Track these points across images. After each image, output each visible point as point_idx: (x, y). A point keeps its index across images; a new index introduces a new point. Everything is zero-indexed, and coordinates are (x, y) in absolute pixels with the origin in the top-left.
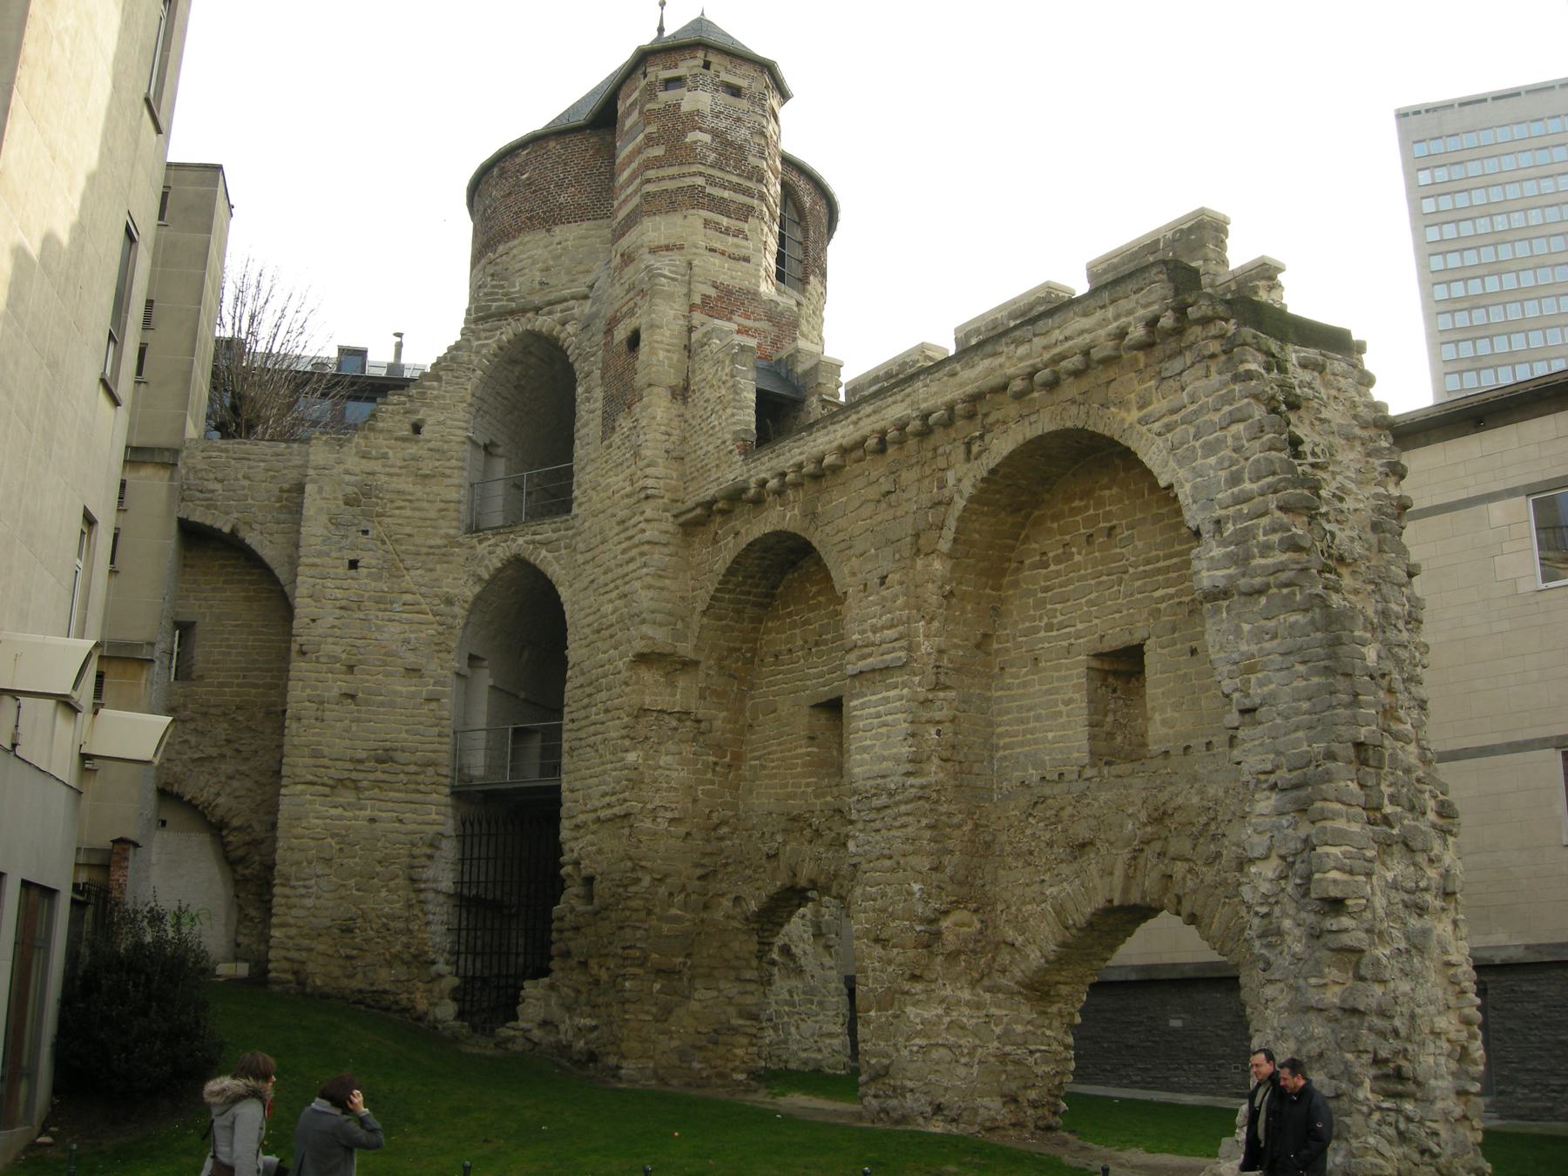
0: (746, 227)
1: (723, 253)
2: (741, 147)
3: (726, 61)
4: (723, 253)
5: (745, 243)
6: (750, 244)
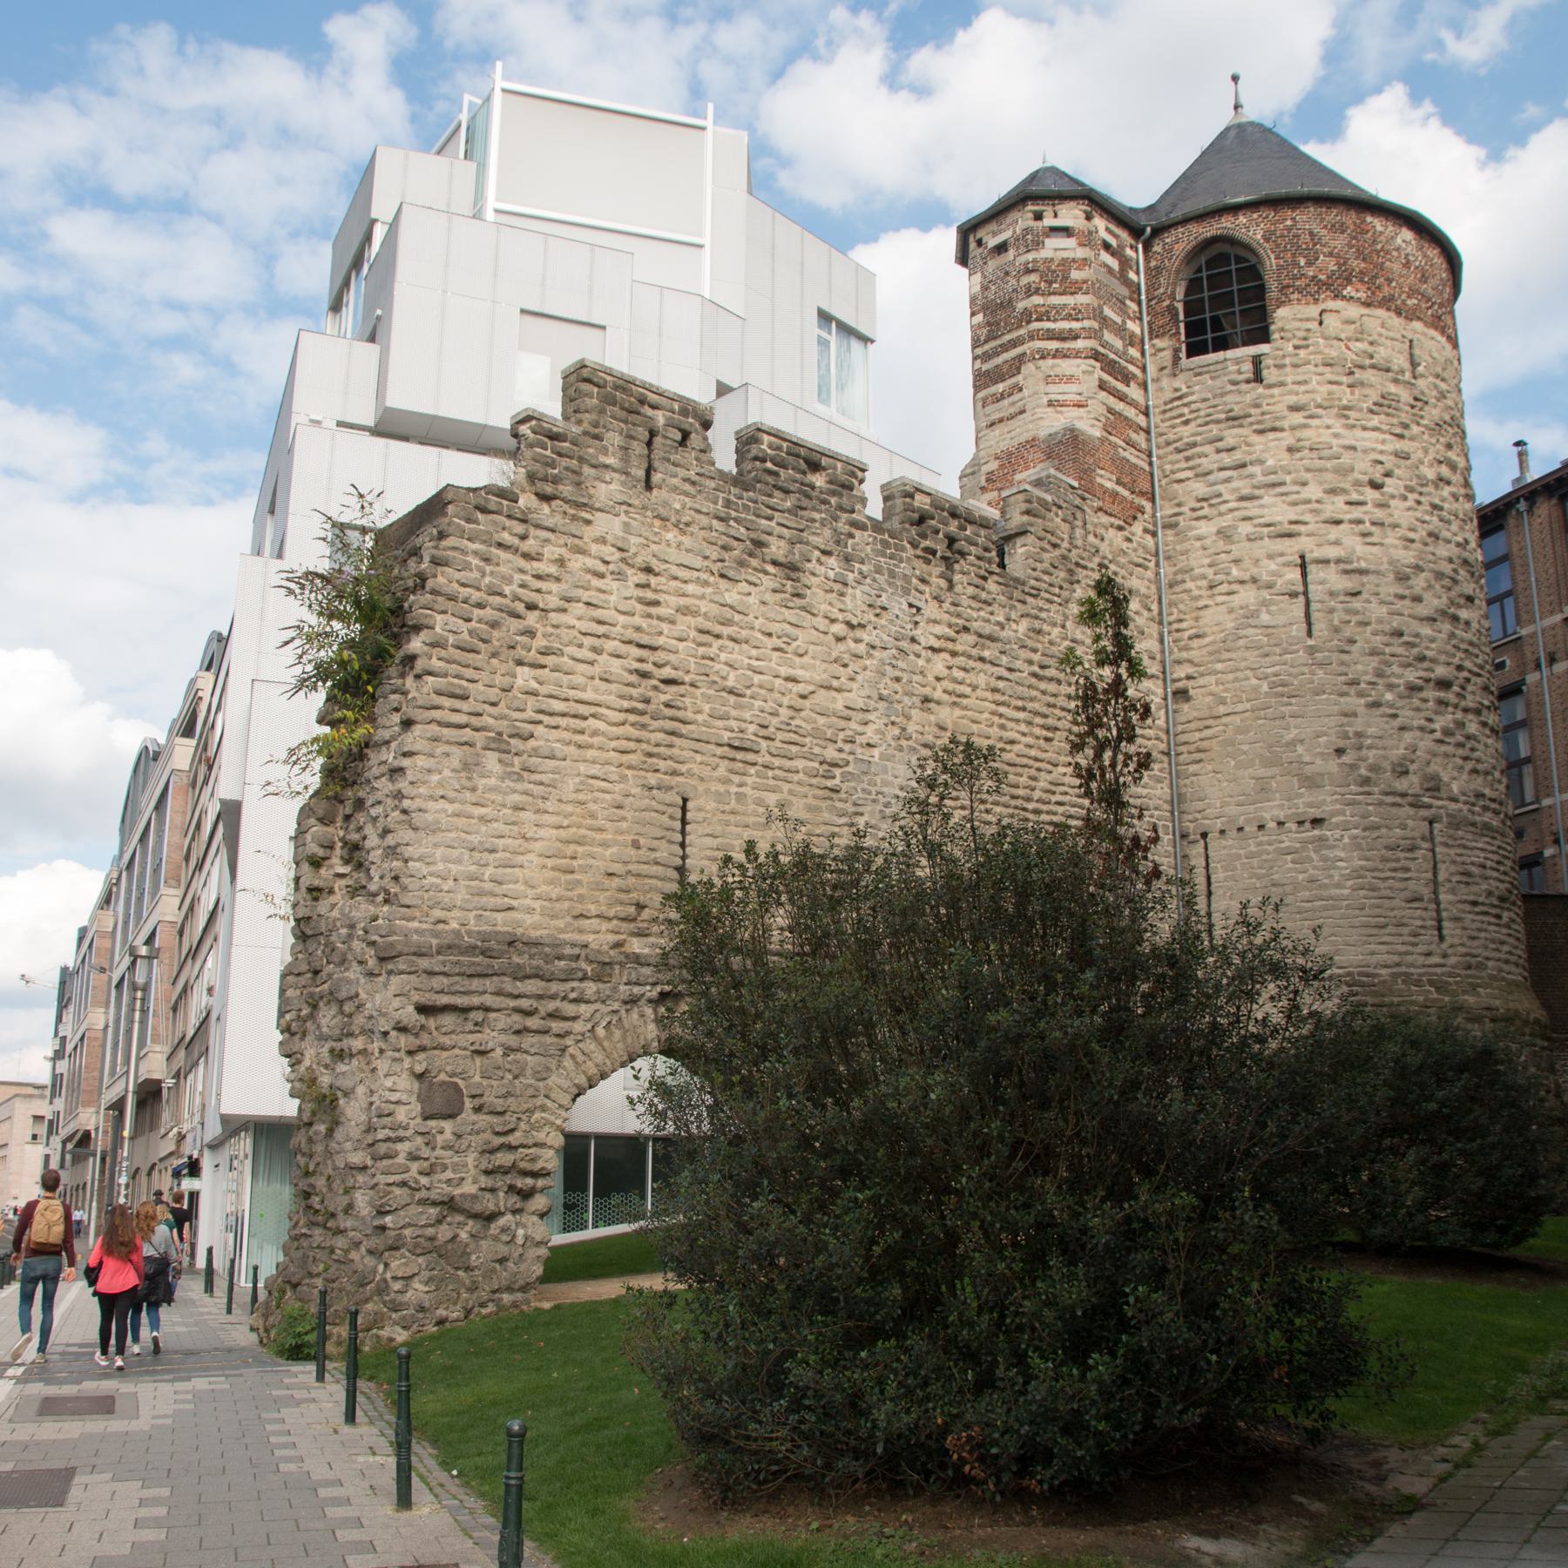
0: (1020, 378)
1: (1001, 421)
2: (1010, 301)
3: (993, 226)
4: (1001, 421)
5: (1020, 395)
6: (1026, 392)
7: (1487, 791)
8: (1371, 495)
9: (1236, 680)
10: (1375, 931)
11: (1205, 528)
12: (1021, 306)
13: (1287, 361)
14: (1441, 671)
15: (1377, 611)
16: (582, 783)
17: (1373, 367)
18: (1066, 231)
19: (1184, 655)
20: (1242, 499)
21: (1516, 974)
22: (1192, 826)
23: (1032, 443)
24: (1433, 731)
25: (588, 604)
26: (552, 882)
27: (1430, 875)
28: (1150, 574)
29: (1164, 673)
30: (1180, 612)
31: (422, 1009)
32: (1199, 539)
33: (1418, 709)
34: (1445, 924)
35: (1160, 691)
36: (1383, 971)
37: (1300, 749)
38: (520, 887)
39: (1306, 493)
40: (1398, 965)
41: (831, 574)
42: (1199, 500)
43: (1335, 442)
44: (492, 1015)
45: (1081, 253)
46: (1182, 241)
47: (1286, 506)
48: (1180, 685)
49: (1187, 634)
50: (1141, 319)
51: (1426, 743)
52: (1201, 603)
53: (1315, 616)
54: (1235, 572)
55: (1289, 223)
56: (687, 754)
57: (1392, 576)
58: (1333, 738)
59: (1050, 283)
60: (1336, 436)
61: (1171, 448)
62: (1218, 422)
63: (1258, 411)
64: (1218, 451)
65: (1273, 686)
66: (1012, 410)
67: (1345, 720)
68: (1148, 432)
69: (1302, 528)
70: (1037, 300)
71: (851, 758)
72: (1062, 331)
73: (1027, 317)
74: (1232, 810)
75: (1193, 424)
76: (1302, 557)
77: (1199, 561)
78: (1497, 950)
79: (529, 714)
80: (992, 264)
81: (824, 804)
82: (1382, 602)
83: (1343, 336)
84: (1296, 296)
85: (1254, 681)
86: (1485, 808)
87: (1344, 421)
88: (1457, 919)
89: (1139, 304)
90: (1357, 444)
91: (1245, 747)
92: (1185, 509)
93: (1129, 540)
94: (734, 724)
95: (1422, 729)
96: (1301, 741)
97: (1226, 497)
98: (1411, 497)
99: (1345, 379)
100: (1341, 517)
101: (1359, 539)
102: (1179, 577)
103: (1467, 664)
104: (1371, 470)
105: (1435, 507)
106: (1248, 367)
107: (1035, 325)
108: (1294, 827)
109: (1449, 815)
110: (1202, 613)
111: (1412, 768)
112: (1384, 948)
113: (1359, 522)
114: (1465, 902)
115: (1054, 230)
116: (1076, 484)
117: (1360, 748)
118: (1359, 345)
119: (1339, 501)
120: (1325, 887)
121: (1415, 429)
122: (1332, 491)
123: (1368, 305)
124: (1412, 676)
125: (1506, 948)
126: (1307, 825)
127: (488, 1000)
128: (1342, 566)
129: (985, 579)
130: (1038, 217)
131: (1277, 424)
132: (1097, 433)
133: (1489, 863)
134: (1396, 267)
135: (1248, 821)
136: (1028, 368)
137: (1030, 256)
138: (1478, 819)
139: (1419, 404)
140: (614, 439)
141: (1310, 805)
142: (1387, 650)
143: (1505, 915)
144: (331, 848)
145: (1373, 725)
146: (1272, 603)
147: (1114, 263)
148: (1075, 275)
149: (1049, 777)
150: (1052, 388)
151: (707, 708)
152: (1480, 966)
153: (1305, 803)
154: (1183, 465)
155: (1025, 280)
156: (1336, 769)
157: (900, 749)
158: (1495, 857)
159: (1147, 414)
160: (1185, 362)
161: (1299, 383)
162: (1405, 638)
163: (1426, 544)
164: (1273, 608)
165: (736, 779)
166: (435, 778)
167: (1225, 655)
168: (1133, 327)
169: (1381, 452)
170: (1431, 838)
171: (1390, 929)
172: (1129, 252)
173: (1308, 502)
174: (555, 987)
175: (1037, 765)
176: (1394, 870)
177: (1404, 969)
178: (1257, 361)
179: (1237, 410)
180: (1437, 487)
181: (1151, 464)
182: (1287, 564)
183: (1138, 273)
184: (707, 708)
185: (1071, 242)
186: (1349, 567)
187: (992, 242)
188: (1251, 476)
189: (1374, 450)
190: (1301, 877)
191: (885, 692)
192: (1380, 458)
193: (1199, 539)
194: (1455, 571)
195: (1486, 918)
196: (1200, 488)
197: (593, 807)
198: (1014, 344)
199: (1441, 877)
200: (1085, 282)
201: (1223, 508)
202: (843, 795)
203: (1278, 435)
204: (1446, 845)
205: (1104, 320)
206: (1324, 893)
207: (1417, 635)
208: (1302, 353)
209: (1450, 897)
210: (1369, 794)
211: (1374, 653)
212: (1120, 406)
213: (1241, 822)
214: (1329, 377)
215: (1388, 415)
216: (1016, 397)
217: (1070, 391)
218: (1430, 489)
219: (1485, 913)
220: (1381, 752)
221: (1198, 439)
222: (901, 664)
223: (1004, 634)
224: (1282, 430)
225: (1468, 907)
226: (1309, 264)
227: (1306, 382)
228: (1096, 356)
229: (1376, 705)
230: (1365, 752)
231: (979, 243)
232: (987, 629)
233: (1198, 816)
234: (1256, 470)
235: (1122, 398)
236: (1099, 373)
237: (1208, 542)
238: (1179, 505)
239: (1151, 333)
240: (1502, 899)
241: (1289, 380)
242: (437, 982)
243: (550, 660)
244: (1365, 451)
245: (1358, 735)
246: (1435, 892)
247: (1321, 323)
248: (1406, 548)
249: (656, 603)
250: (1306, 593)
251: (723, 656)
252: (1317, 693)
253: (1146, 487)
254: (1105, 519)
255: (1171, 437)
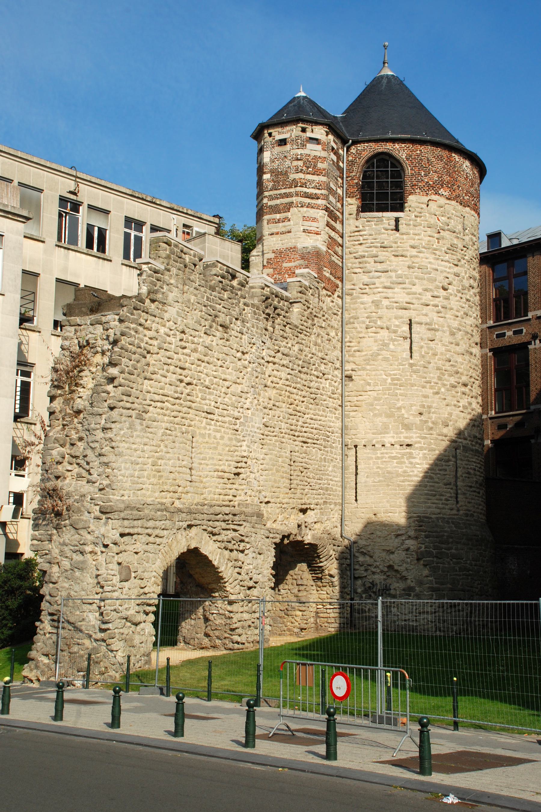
0: (289, 215)
1: (277, 234)
4: (277, 234)
5: (289, 223)
6: (292, 222)
7: (477, 435)
8: (443, 293)
9: (376, 375)
10: (430, 497)
11: (365, 298)
12: (292, 176)
13: (411, 222)
14: (464, 379)
15: (441, 349)
16: (164, 432)
17: (448, 230)
18: (316, 141)
19: (351, 359)
20: (385, 287)
21: (483, 518)
22: (350, 441)
23: (294, 249)
24: (459, 407)
25: (165, 350)
26: (154, 476)
27: (454, 473)
28: (339, 318)
29: (342, 366)
30: (350, 337)
31: (122, 535)
32: (362, 303)
33: (454, 397)
34: (459, 496)
35: (340, 376)
36: (433, 516)
37: (403, 411)
38: (145, 479)
39: (414, 289)
40: (439, 514)
41: (238, 329)
42: (364, 285)
43: (429, 266)
44: (140, 536)
45: (324, 154)
46: (367, 150)
47: (405, 295)
48: (347, 373)
49: (353, 349)
50: (343, 187)
51: (456, 412)
52: (361, 335)
53: (414, 348)
54: (379, 323)
55: (418, 152)
56: (194, 416)
57: (448, 333)
58: (418, 408)
59: (308, 168)
60: (430, 263)
61: (352, 256)
62: (376, 247)
63: (396, 245)
64: (375, 262)
65: (393, 379)
66: (284, 230)
67: (424, 399)
68: (342, 247)
69: (412, 306)
70: (301, 175)
71: (242, 415)
72: (311, 194)
73: (295, 183)
74: (370, 436)
75: (364, 245)
76: (410, 320)
77: (363, 315)
78: (478, 508)
79: (148, 402)
80: (278, 149)
81: (234, 437)
82: (444, 345)
83: (437, 213)
84: (418, 191)
85: (384, 377)
86: (477, 443)
87: (434, 256)
88: (464, 494)
89: (343, 179)
90: (439, 268)
91: (378, 407)
92: (357, 287)
93: (333, 302)
94: (207, 402)
95: (455, 405)
96: (404, 407)
97: (377, 285)
98: (460, 295)
99: (436, 235)
100: (428, 303)
101: (436, 314)
102: (352, 320)
103: (474, 375)
104: (443, 281)
105: (468, 300)
106: (393, 223)
107: (299, 189)
108: (398, 447)
109: (463, 446)
110: (361, 340)
111: (451, 423)
112: (434, 505)
113: (437, 306)
114: (468, 486)
115: (311, 139)
116: (316, 276)
117: (429, 413)
118: (443, 218)
119: (429, 295)
120: (410, 476)
121: (463, 262)
122: (426, 290)
123: (448, 199)
124: (452, 380)
125: (481, 507)
126: (404, 446)
127: (139, 530)
128: (427, 326)
129: (285, 326)
130: (304, 130)
131: (404, 253)
132: (324, 248)
133: (477, 468)
134: (462, 180)
135: (378, 442)
136: (293, 210)
137: (299, 152)
138: (474, 448)
139: (465, 249)
140: (174, 271)
141: (406, 438)
142: (444, 368)
143: (481, 492)
144: (64, 458)
145: (435, 402)
146: (395, 340)
147: (335, 158)
148: (320, 165)
149: (303, 420)
150: (306, 223)
151: (200, 395)
152: (472, 515)
153: (404, 437)
154: (358, 265)
155: (295, 163)
156: (418, 422)
157: (257, 410)
158: (479, 466)
159: (342, 237)
160: (362, 214)
161: (416, 234)
162: (451, 363)
163: (463, 318)
164: (396, 343)
165: (208, 427)
166: (122, 432)
167: (372, 362)
168: (340, 191)
169: (448, 273)
170: (455, 457)
171: (437, 497)
172: (341, 151)
173: (415, 294)
174: (158, 524)
175: (299, 414)
176: (440, 470)
177: (441, 516)
178: (397, 220)
179: (386, 243)
180: (469, 290)
181: (342, 262)
182: (403, 323)
183: (343, 163)
184: (200, 395)
185: (319, 147)
186: (430, 327)
187: (278, 137)
188: (391, 277)
189: (445, 271)
190: (400, 470)
191: (253, 384)
192: (448, 276)
193: (362, 303)
194: (472, 331)
195: (475, 494)
196: (365, 278)
197: (166, 442)
198: (287, 195)
199: (459, 474)
200: (324, 170)
201: (376, 290)
202: (239, 432)
203: (403, 258)
204: (462, 460)
205: (330, 190)
206: (410, 479)
207: (456, 362)
208: (418, 219)
209: (462, 484)
210: (431, 434)
211: (438, 369)
212: (333, 234)
213: (374, 442)
214: (429, 233)
215: (452, 254)
216: (286, 223)
217: (313, 226)
218: (466, 291)
219: (475, 491)
220: (438, 415)
221: (366, 254)
222: (259, 370)
223: (291, 352)
224: (406, 257)
225: (468, 489)
226: (426, 175)
227: (419, 234)
228: (327, 209)
229: (437, 393)
230: (431, 415)
231: (270, 135)
232: (286, 351)
233: (353, 437)
234: (393, 274)
235: (334, 229)
236: (326, 218)
237: (367, 306)
238: (354, 285)
239: (347, 193)
240: (481, 485)
241: (411, 232)
242: (126, 523)
243: (154, 377)
244: (441, 272)
245: (430, 407)
246: (456, 481)
247: (428, 206)
248: (454, 320)
249: (185, 348)
250: (411, 338)
251: (205, 371)
252: (412, 385)
253: (339, 274)
254: (325, 292)
255: (352, 250)
